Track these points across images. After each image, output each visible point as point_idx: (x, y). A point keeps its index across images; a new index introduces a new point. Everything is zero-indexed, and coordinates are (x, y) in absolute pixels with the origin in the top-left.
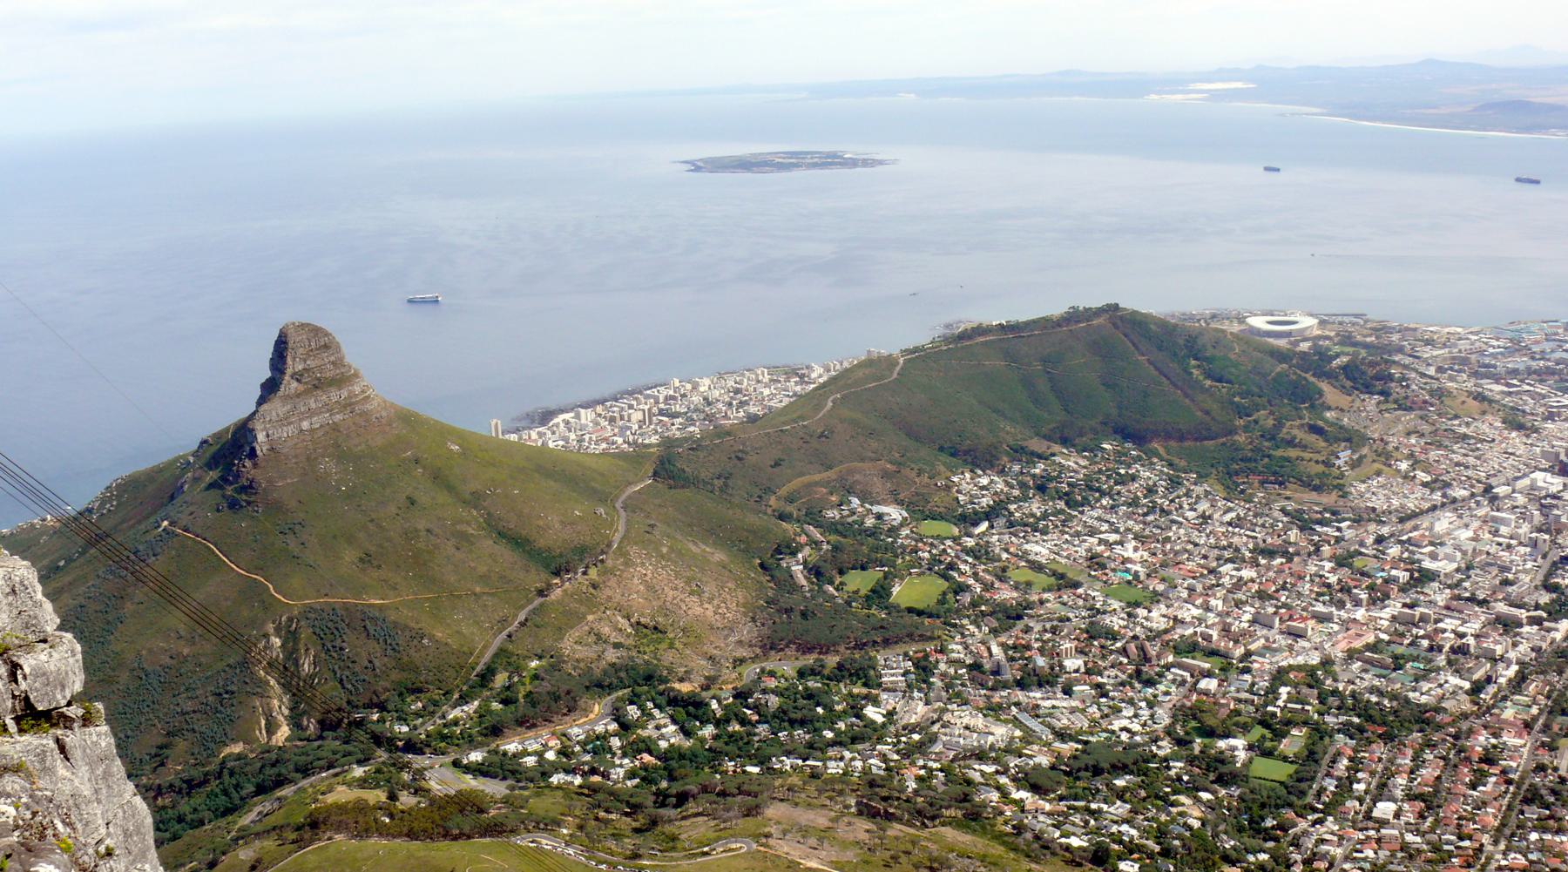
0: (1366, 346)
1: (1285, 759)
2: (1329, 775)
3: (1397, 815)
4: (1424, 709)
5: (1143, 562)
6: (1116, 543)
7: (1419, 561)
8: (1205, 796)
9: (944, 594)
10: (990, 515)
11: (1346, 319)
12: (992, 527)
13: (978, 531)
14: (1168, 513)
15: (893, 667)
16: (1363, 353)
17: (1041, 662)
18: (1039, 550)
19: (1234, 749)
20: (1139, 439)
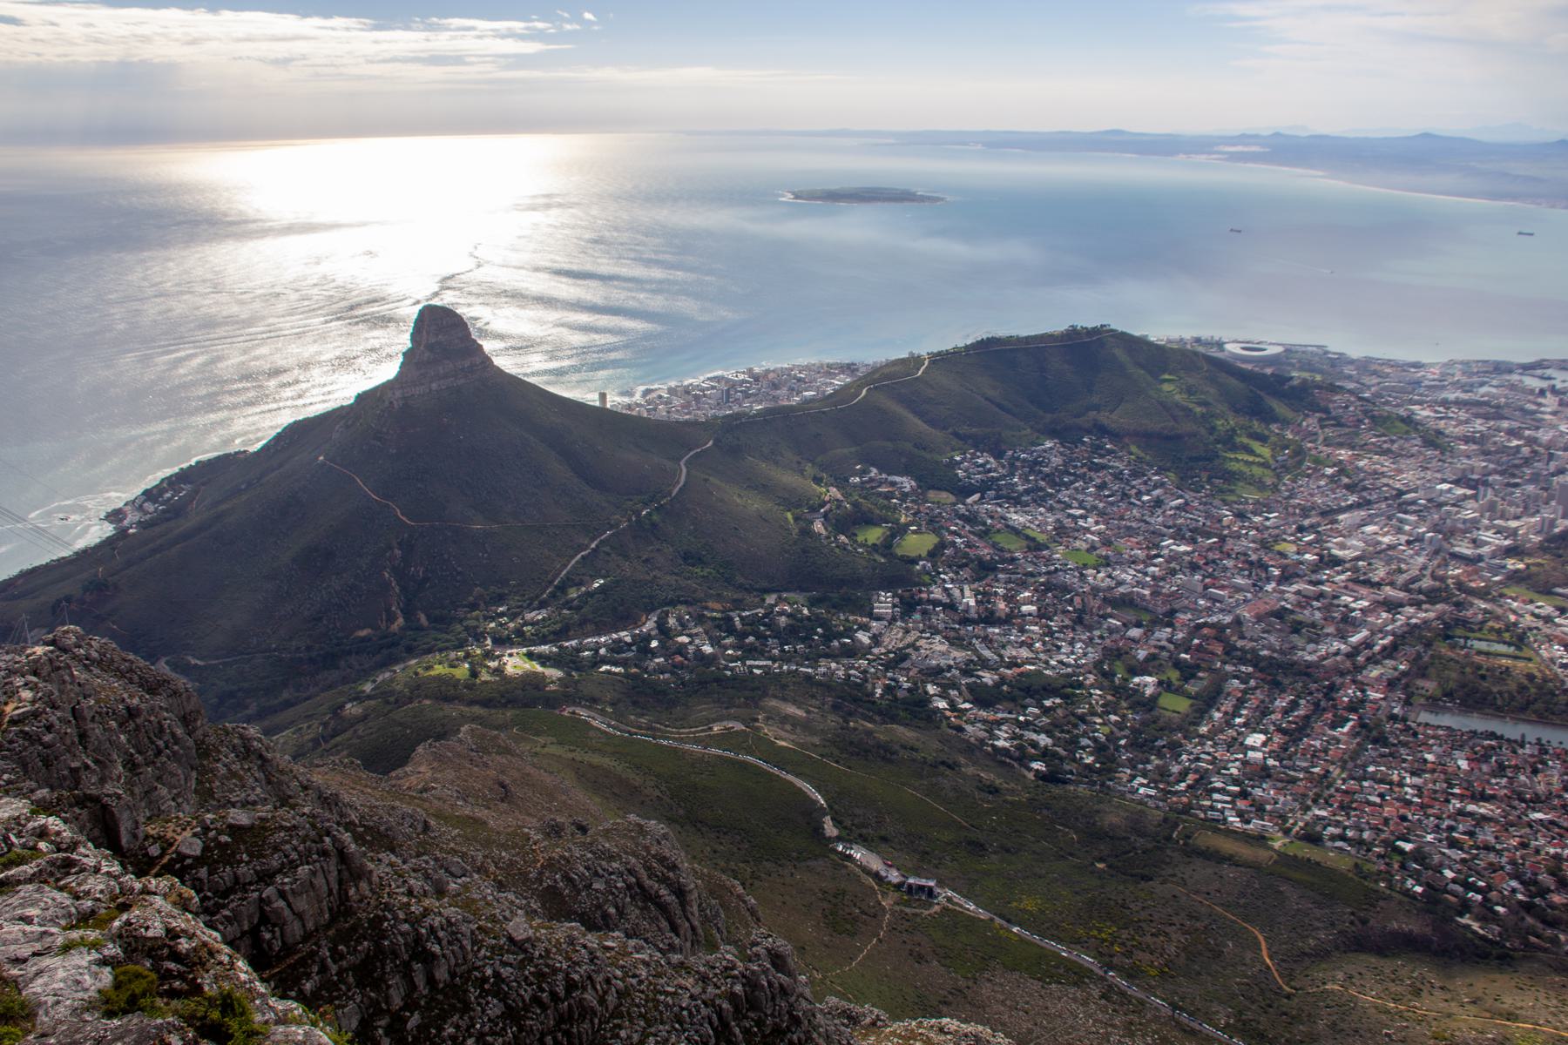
0: (1320, 372)
1: (1189, 697)
3: (1264, 744)
4: (1309, 665)
5: (1099, 533)
6: (1082, 517)
7: (1328, 549)
8: (1113, 718)
9: (936, 547)
10: (983, 488)
12: (982, 497)
13: (969, 500)
14: (1129, 496)
15: (884, 603)
17: (1002, 605)
18: (1017, 518)
20: (1115, 436)
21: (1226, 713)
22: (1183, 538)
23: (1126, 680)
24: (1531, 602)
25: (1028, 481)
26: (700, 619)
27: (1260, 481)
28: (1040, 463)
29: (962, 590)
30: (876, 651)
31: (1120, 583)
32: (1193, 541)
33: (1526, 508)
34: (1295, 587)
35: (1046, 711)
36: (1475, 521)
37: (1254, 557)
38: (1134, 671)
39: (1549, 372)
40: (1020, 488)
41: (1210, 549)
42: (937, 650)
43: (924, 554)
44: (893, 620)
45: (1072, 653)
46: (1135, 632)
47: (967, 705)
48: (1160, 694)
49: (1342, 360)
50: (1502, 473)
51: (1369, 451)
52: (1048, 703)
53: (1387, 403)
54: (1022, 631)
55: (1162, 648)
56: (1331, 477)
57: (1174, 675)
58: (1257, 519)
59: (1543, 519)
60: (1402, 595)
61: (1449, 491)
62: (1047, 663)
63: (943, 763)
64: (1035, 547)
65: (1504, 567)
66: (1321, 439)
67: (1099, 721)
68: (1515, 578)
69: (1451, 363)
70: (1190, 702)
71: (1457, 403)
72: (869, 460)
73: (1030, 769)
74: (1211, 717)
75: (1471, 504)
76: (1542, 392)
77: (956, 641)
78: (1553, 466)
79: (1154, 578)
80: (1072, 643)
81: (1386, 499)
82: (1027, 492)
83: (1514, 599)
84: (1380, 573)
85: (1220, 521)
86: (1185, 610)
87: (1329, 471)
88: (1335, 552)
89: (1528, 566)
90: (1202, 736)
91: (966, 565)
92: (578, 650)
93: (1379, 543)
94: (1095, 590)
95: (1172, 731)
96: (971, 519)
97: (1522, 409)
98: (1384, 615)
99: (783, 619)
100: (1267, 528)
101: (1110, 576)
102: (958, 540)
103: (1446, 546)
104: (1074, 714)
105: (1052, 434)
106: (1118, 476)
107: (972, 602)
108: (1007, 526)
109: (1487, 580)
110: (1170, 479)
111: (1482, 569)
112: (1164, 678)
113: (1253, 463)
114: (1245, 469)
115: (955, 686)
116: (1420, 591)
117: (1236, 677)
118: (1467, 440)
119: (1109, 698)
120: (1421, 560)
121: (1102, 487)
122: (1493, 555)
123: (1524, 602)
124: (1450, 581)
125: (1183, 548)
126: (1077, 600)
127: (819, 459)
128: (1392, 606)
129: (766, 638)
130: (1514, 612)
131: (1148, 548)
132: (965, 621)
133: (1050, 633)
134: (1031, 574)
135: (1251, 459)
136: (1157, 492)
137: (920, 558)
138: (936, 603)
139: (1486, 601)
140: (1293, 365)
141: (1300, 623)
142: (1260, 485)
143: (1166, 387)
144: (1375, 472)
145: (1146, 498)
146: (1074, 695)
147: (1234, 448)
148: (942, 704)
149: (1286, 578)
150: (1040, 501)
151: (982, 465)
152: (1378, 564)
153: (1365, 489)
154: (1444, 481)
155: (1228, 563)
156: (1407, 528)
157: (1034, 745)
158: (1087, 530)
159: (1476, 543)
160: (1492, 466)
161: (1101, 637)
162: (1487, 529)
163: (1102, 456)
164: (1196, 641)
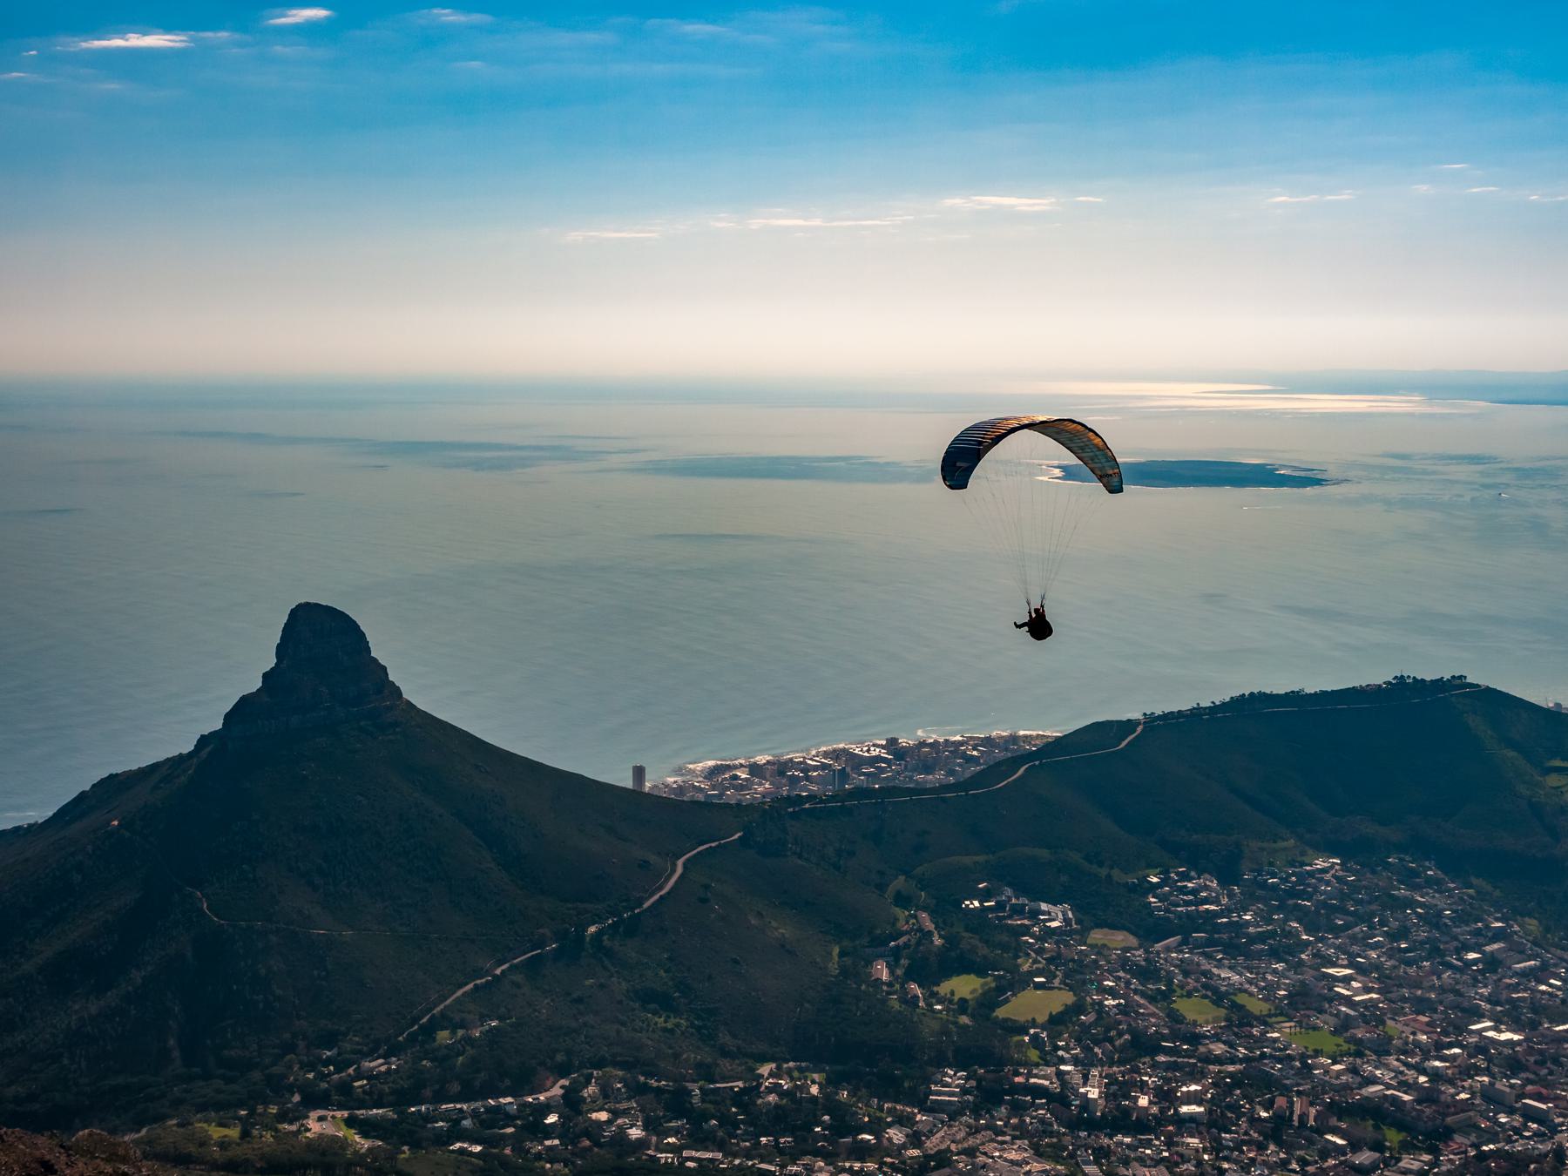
10: (1185, 927)
12: (1185, 942)
13: (1158, 946)
15: (951, 1083)
25: (1270, 921)
26: (637, 1090)
32: (1534, 1025)
40: (1251, 930)
43: (1042, 1018)
72: (1003, 874)
79: (1435, 1076)
82: (1261, 938)
92: (429, 1118)
99: (772, 1098)
102: (1110, 1002)
106: (1433, 919)
121: (1393, 936)
126: (1281, 1102)
127: (919, 870)
129: (736, 1125)
132: (1074, 1125)
134: (1219, 1060)
137: (1034, 1024)
138: (1038, 1091)
145: (1472, 956)
151: (1194, 892)
158: (1347, 1001)
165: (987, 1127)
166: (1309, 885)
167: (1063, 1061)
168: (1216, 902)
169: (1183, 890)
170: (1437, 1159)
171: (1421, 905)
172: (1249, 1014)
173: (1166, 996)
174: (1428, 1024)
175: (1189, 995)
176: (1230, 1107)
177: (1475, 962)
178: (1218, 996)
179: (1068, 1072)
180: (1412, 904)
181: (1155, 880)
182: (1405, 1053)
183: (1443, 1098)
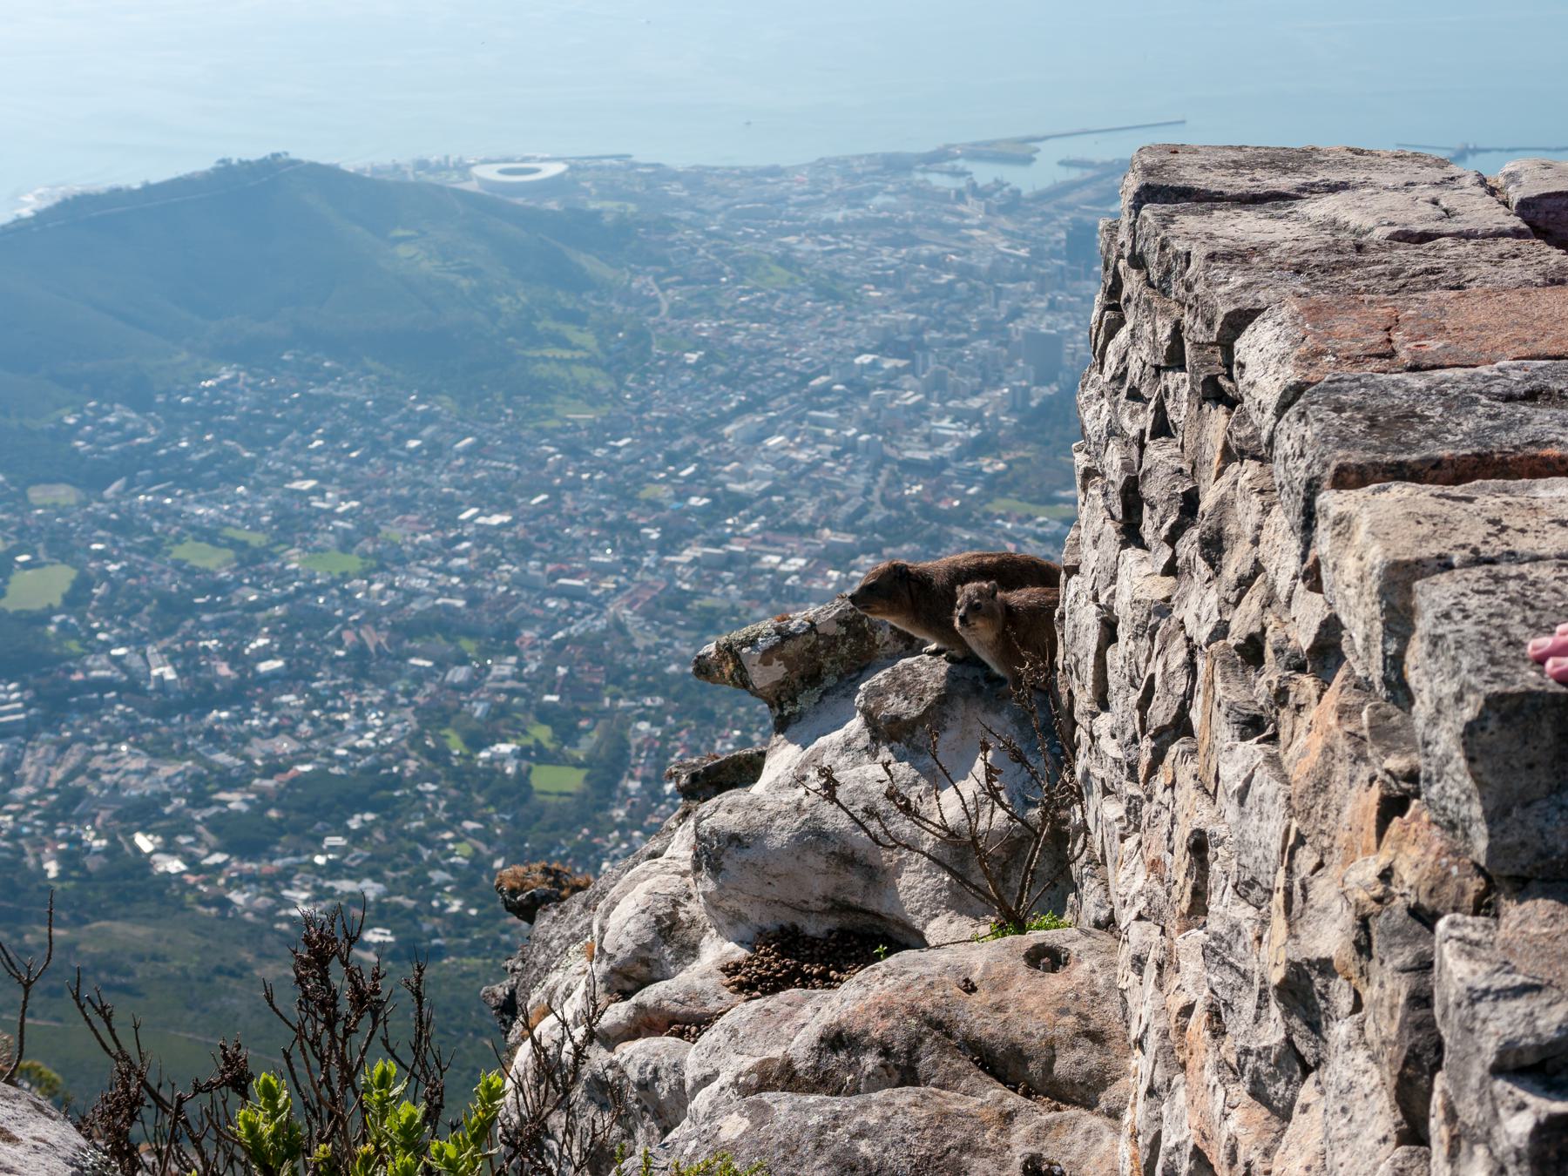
2: (632, 777)
6: (313, 491)
7: (722, 484)
8: (469, 825)
9: (74, 583)
11: (606, 162)
13: (109, 493)
16: (632, 207)
17: (224, 669)
19: (503, 759)
21: (645, 780)
22: (492, 502)
23: (469, 758)
24: (1030, 518)
25: (207, 445)
27: (591, 388)
28: (220, 410)
29: (144, 656)
30: (21, 792)
31: (414, 594)
33: (984, 377)
34: (688, 555)
35: (356, 838)
36: (919, 408)
37: (611, 516)
38: (476, 741)
39: (960, 163)
40: (195, 457)
41: (539, 512)
42: (129, 767)
43: (57, 602)
44: (29, 731)
45: (366, 728)
46: (459, 674)
47: (218, 858)
48: (529, 770)
49: (660, 173)
50: (939, 326)
51: (741, 317)
52: (354, 824)
53: (747, 237)
54: (271, 708)
55: (512, 692)
56: (697, 367)
57: (543, 733)
58: (599, 452)
59: (1014, 390)
60: (849, 539)
61: (874, 365)
62: (329, 755)
63: (219, 971)
64: (250, 559)
65: (980, 472)
66: (665, 307)
67: (448, 835)
68: (995, 486)
69: (822, 165)
70: (583, 772)
71: (847, 225)
73: (367, 946)
74: (625, 791)
75: (908, 380)
76: (960, 196)
77: (160, 750)
78: (1005, 304)
79: (463, 573)
80: (360, 712)
81: (786, 391)
82: (207, 464)
83: (1005, 518)
84: (808, 510)
85: (542, 463)
86: (529, 620)
87: (692, 358)
88: (734, 487)
89: (1009, 463)
90: (621, 827)
91: (138, 609)
93: (794, 462)
94: (373, 616)
95: (572, 827)
96: (125, 526)
97: (939, 225)
98: (834, 574)
100: (620, 464)
101: (391, 586)
102: (113, 567)
103: (892, 452)
104: (404, 834)
105: (227, 354)
107: (169, 674)
108: (192, 528)
109: (961, 495)
110: (445, 405)
111: (950, 480)
112: (529, 742)
113: (572, 361)
114: (561, 372)
115: (187, 827)
116: (873, 528)
117: (642, 718)
118: (879, 282)
119: (453, 792)
120: (859, 480)
122: (959, 456)
123: (1020, 520)
124: (911, 505)
125: (496, 520)
126: (348, 637)
128: (839, 558)
130: (1011, 538)
131: (440, 528)
132: (164, 712)
133: (318, 701)
135: (567, 354)
136: (428, 431)
137: (52, 611)
138: (103, 685)
139: (968, 527)
140: (586, 191)
141: (712, 610)
142: (594, 399)
143: (403, 251)
144: (760, 351)
145: (413, 444)
146: (396, 800)
147: (537, 340)
148: (175, 865)
149: (669, 544)
150: (239, 473)
151: (118, 427)
152: (800, 495)
153: (753, 379)
154: (861, 351)
155: (576, 532)
156: (828, 432)
157: (359, 900)
158: (331, 514)
159: (931, 441)
160: (922, 318)
161: (408, 694)
162: (941, 417)
163: (321, 382)
164: (562, 671)
165: (74, 740)
166: (225, 398)
167: (107, 646)
168: (144, 434)
169: (108, 428)
170: (521, 658)
171: (345, 400)
172: (256, 551)
173: (154, 548)
174: (419, 522)
175: (178, 540)
176: (302, 654)
177: (419, 449)
178: (209, 535)
179: (123, 657)
180: (331, 402)
181: (71, 421)
182: (424, 557)
183: (486, 595)
